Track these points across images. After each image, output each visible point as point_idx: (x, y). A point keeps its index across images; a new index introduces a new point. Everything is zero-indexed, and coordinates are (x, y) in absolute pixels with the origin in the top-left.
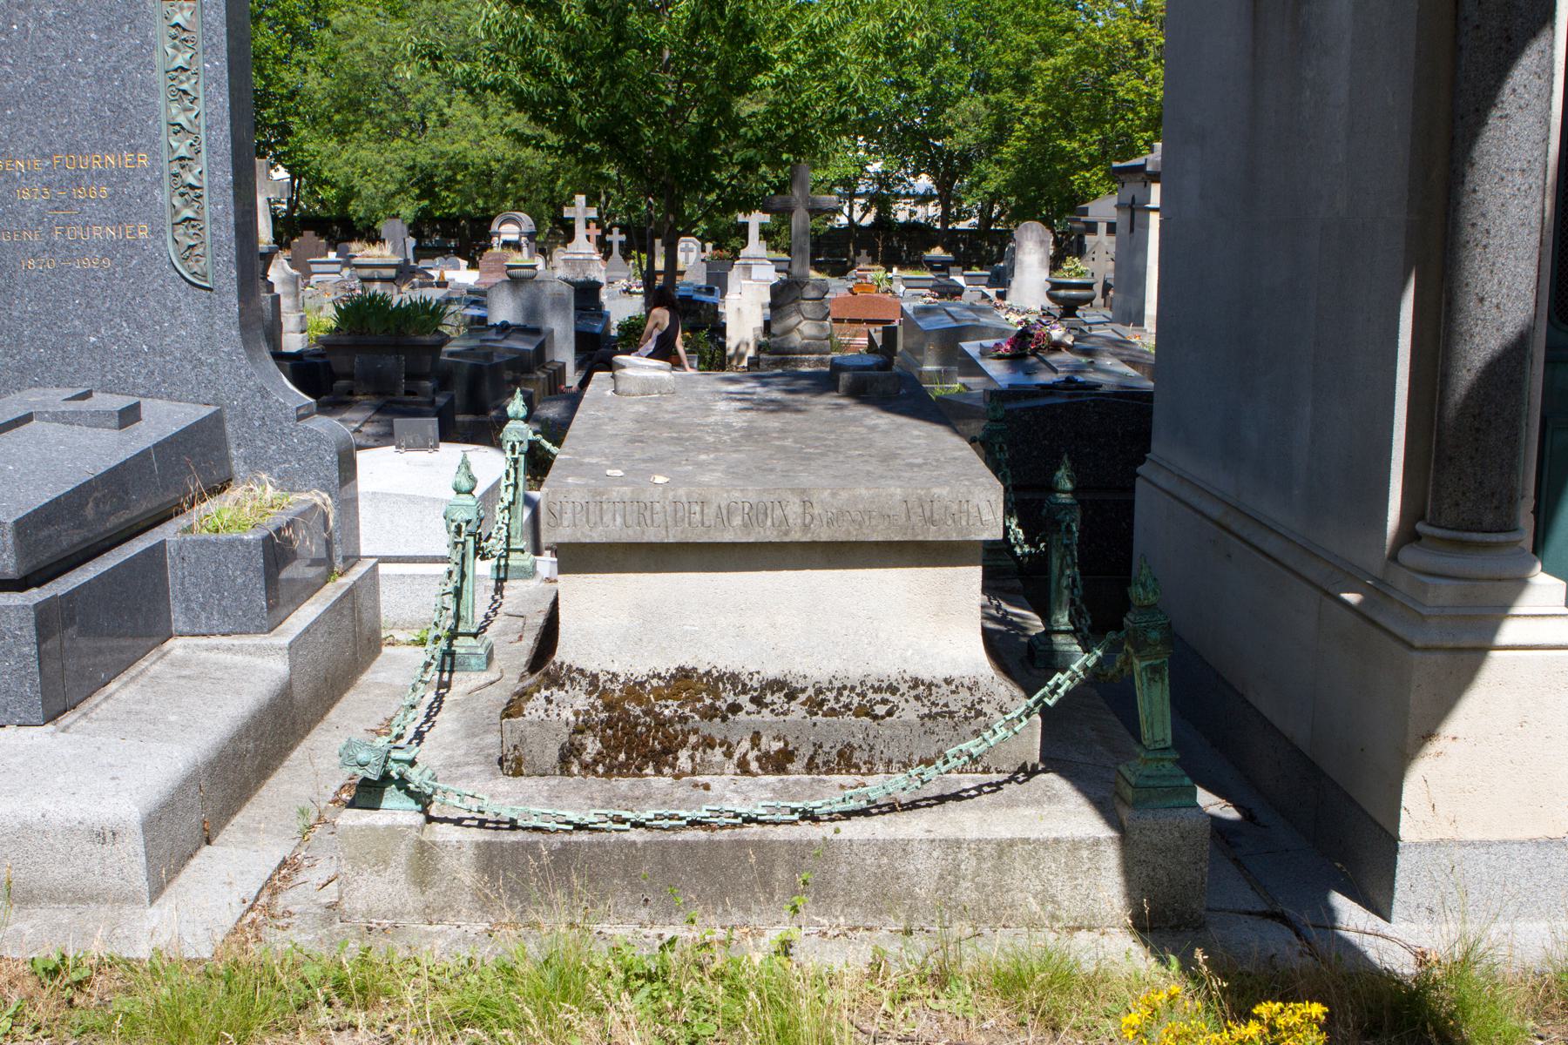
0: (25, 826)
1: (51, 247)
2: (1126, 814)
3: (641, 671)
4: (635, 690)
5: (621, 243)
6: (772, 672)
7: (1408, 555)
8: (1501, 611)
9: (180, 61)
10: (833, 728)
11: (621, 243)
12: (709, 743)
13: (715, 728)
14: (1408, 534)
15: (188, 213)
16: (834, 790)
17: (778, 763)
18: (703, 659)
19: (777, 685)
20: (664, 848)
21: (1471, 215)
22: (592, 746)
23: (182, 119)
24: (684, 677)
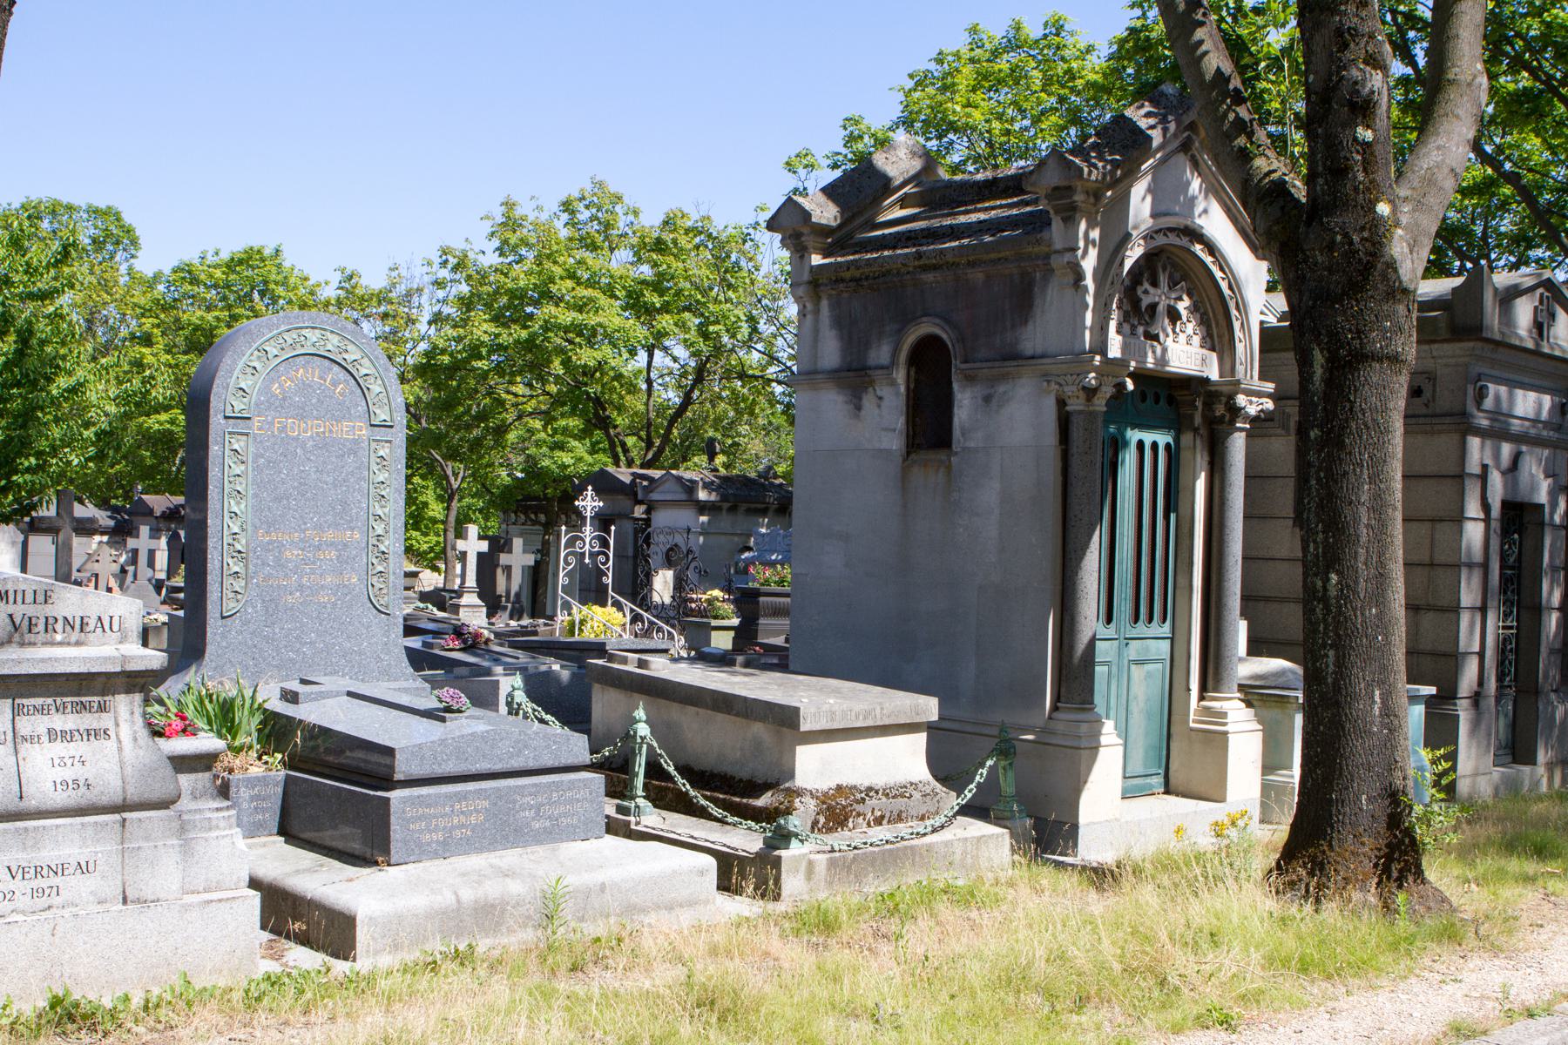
0: (674, 872)
1: (301, 588)
2: (1008, 823)
3: (825, 788)
4: (826, 794)
5: (480, 555)
6: (867, 784)
7: (1055, 715)
8: (1099, 733)
9: (381, 478)
10: (891, 804)
11: (480, 555)
12: (859, 815)
13: (859, 808)
14: (1055, 708)
15: (380, 568)
16: (903, 829)
17: (879, 821)
18: (847, 780)
19: (870, 789)
20: (883, 853)
21: (1081, 587)
22: (822, 820)
23: (380, 512)
24: (839, 788)
